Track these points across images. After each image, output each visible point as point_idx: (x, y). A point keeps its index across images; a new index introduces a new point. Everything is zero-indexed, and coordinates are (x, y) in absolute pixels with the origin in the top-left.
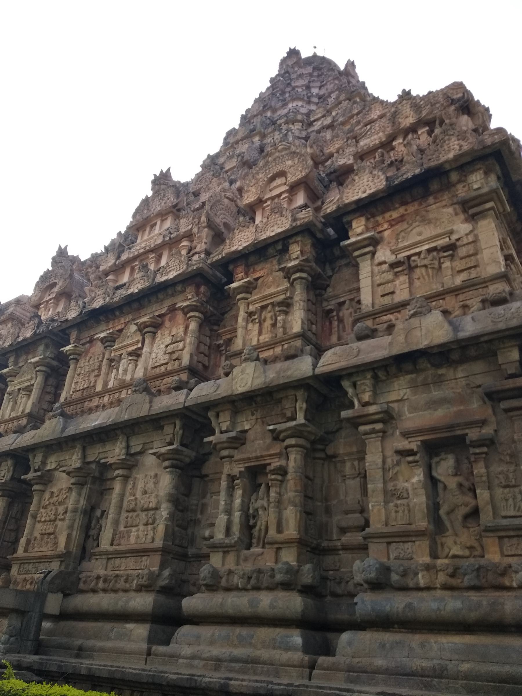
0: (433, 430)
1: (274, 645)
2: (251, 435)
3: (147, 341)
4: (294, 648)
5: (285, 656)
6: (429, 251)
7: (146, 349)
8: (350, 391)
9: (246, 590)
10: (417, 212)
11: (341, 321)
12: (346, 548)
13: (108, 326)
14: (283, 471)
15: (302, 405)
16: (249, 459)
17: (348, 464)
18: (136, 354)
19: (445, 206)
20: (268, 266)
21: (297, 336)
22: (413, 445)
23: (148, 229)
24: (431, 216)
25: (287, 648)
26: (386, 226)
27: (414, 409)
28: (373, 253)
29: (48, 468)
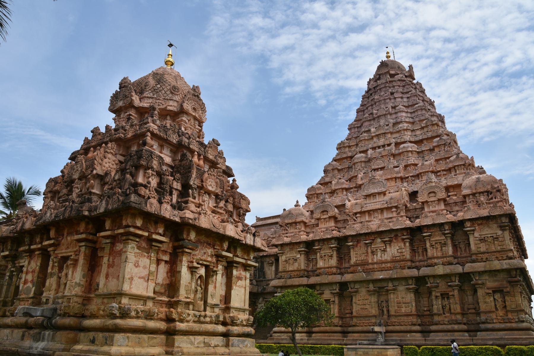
0: (495, 288)
1: (460, 336)
2: (440, 285)
3: (388, 246)
4: (466, 336)
5: (465, 338)
6: (490, 237)
7: (388, 249)
8: (472, 276)
9: (447, 324)
10: (486, 223)
11: (460, 248)
12: (470, 313)
13: (366, 237)
14: (453, 295)
15: (457, 278)
16: (442, 292)
17: (468, 292)
18: (385, 251)
19: (494, 223)
20: (435, 228)
21: (451, 256)
22: (491, 291)
23: (372, 197)
24: (491, 226)
25: (464, 336)
26: (476, 225)
27: (489, 282)
28: (473, 234)
29: (356, 287)
